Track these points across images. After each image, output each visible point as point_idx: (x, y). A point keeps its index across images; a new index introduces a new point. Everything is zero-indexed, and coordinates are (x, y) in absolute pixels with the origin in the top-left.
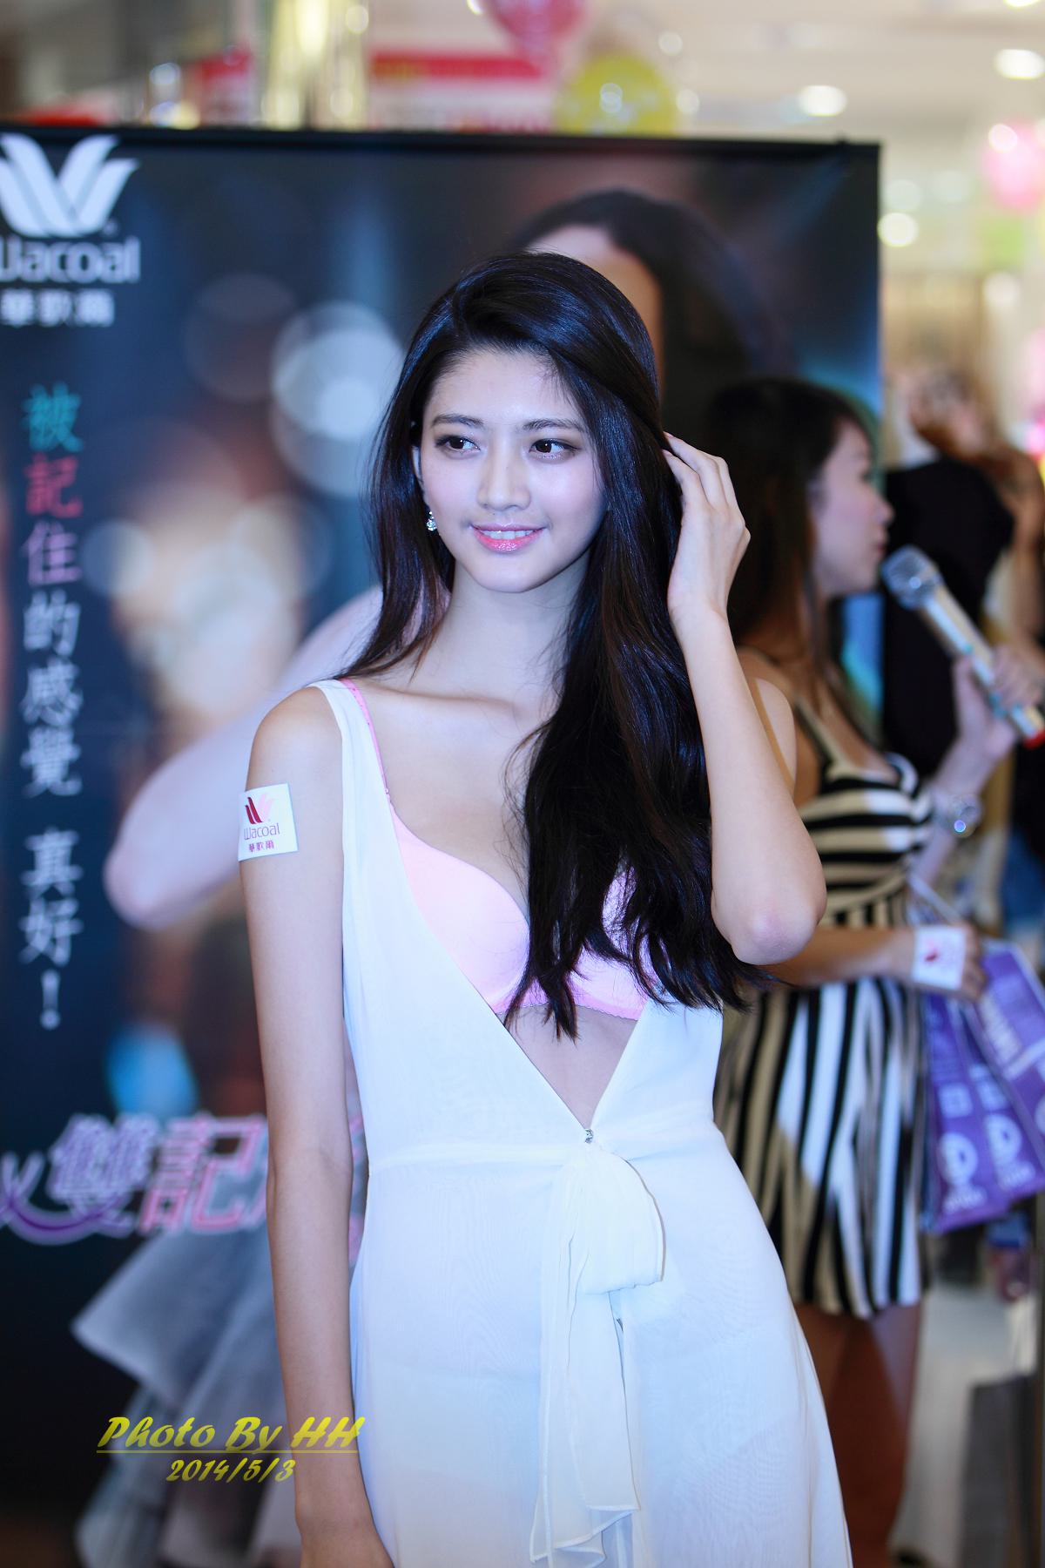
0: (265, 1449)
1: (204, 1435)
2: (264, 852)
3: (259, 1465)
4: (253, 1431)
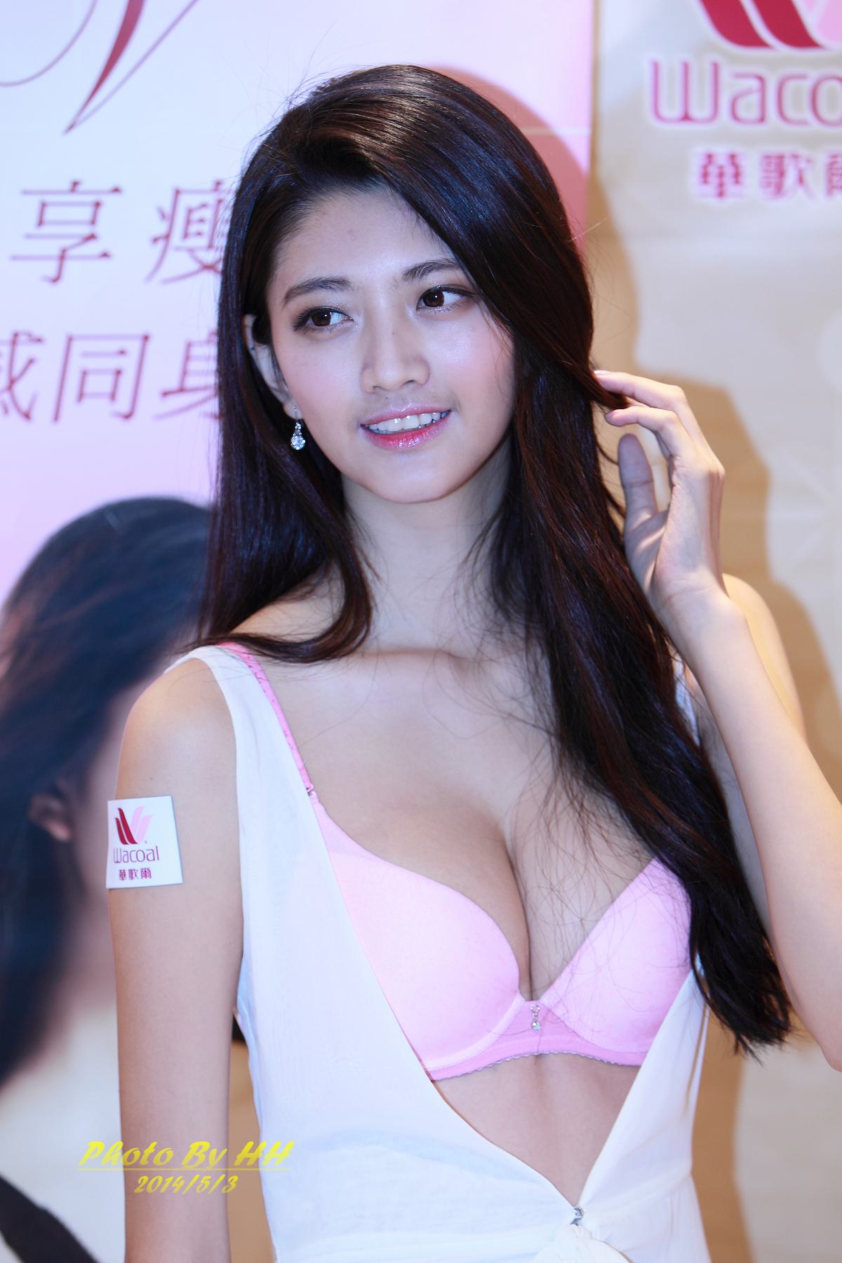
0: (214, 1167)
1: (164, 1156)
2: (139, 882)
3: (209, 1180)
4: (204, 1153)
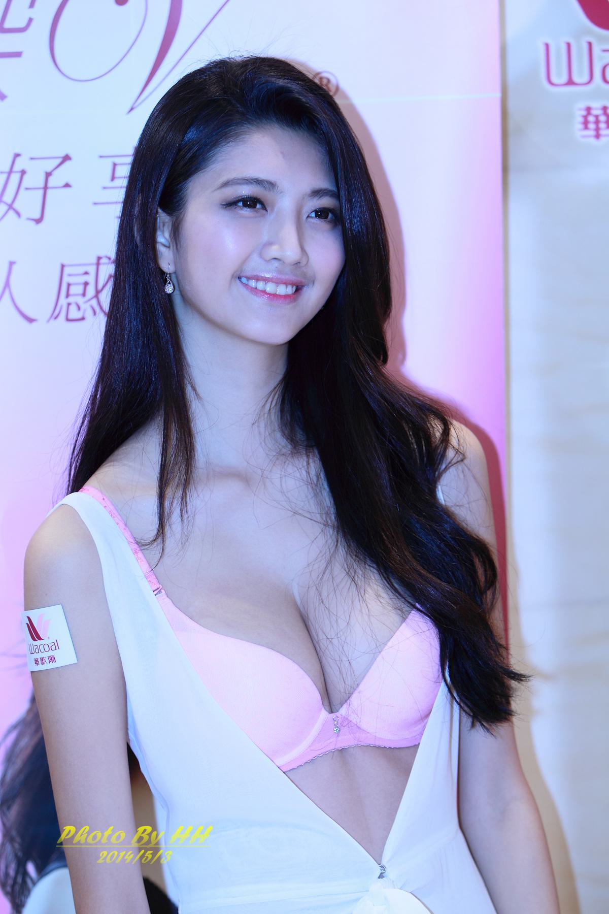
0: (155, 845)
2: (48, 666)
3: (151, 854)
4: (148, 834)
